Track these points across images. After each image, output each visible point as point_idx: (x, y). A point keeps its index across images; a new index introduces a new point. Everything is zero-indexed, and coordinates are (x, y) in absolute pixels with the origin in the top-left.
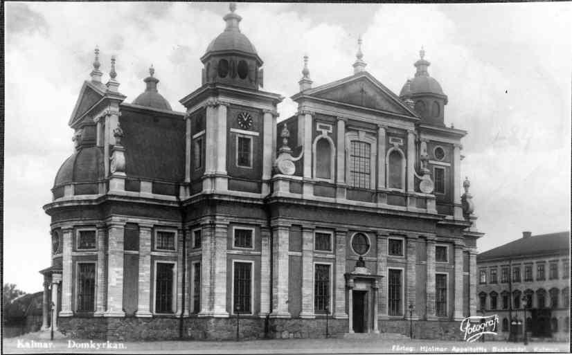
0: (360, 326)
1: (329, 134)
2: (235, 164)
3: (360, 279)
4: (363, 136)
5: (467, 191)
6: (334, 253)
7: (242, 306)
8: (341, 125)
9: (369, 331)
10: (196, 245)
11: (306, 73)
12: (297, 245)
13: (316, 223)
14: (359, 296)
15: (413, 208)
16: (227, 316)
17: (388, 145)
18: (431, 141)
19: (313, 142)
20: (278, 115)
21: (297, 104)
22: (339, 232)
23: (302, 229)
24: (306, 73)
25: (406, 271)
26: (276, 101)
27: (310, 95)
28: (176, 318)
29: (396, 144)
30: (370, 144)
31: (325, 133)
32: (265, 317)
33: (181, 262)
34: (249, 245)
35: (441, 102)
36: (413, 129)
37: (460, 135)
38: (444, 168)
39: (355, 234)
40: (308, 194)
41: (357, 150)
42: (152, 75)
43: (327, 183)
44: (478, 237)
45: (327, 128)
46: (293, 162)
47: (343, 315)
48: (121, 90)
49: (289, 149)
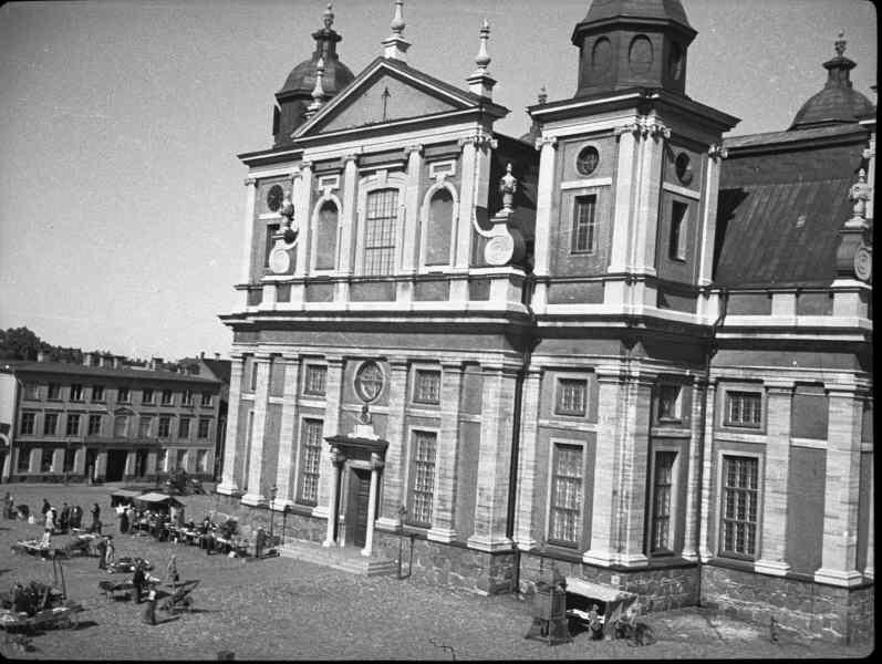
1: (334, 191)
4: (379, 179)
8: (351, 168)
12: (275, 389)
15: (458, 298)
17: (426, 181)
18: (559, 138)
19: (311, 213)
27: (305, 135)
29: (441, 175)
30: (397, 190)
31: (327, 196)
38: (598, 192)
40: (297, 301)
42: (840, 53)
45: (333, 181)
46: (287, 251)
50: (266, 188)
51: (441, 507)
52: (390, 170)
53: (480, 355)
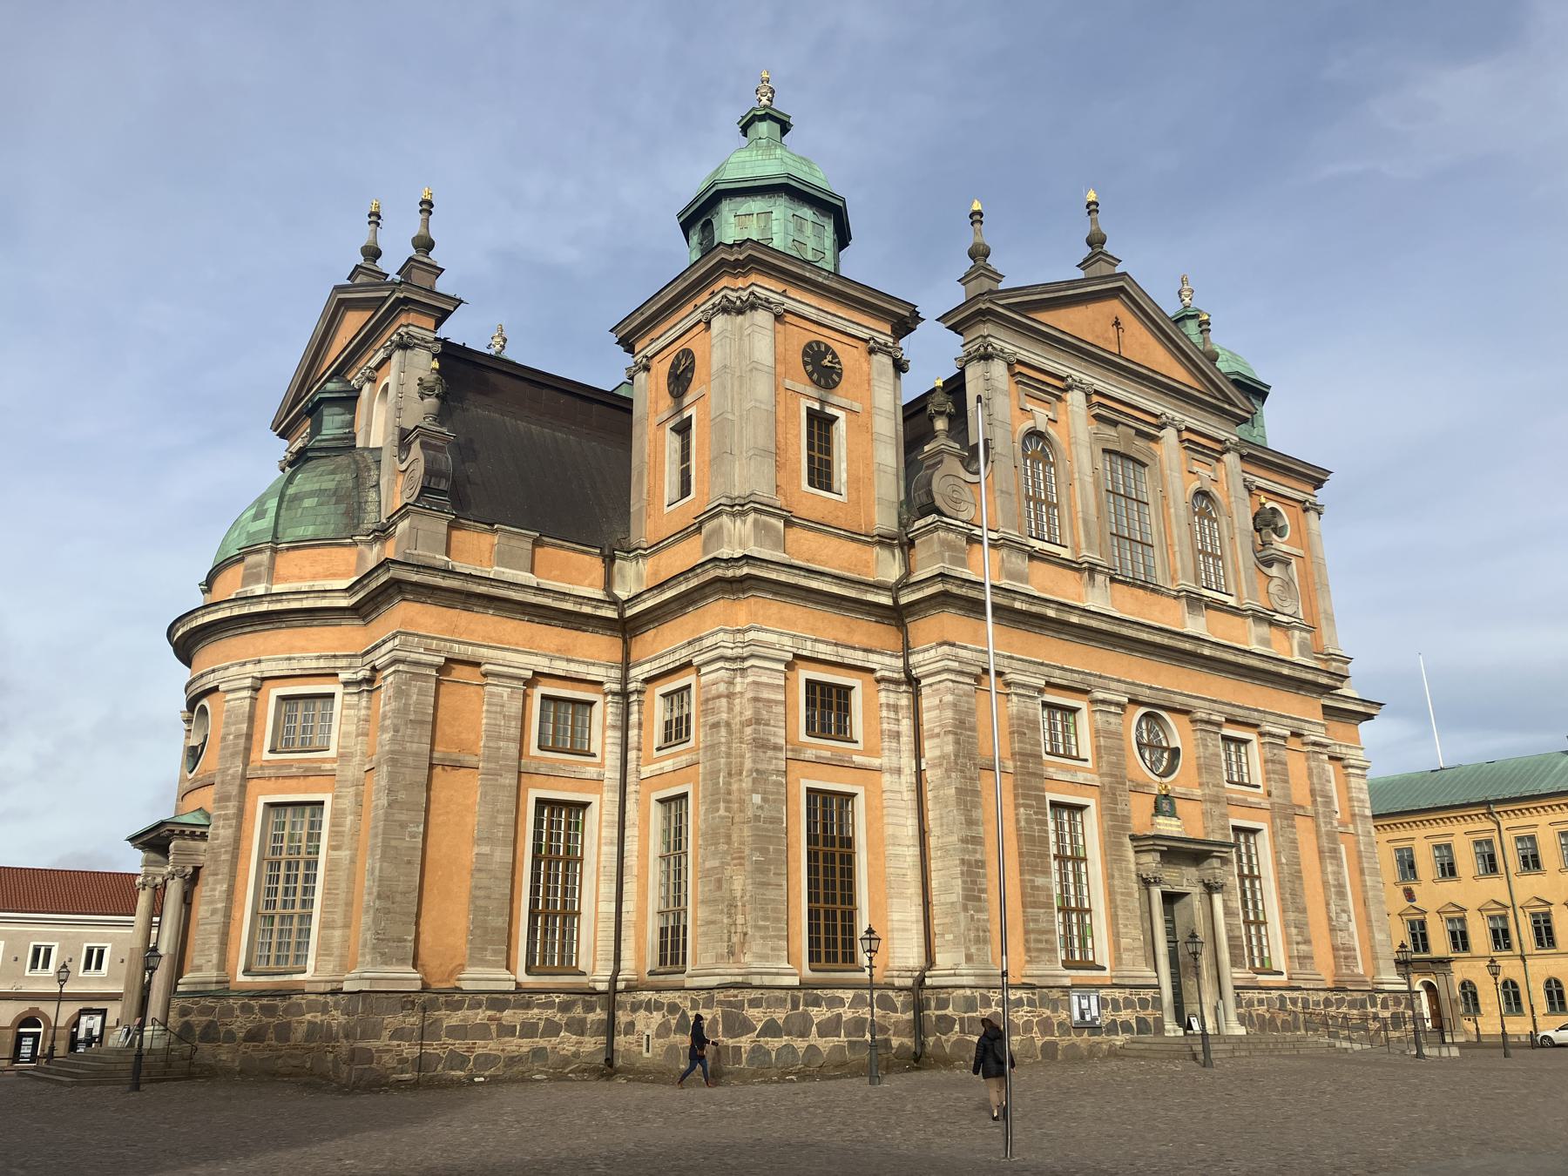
2: (799, 486)
7: (830, 943)
10: (667, 738)
13: (1045, 670)
16: (795, 981)
22: (1103, 702)
24: (979, 253)
25: (1274, 834)
26: (905, 322)
27: (1003, 306)
28: (594, 992)
32: (909, 982)
33: (611, 797)
34: (842, 732)
39: (1144, 710)
43: (1057, 556)
49: (958, 446)
50: (800, 336)
51: (1299, 939)
52: (1139, 433)
53: (1307, 726)
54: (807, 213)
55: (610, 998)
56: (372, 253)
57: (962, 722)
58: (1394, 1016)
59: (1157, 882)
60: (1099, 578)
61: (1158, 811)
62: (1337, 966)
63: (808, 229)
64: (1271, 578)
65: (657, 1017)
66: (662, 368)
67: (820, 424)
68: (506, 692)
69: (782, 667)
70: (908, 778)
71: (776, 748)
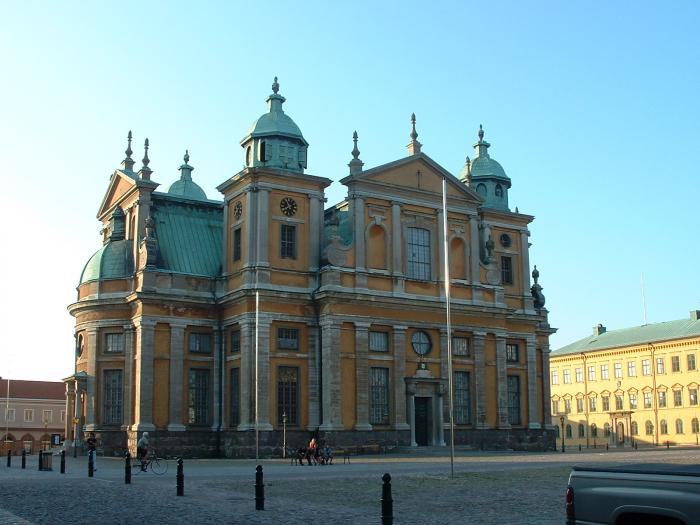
0: (423, 439)
3: (422, 382)
5: (536, 282)
6: (393, 355)
8: (396, 209)
9: (434, 442)
11: (356, 153)
14: (423, 403)
20: (326, 200)
21: (346, 188)
23: (355, 327)
24: (356, 153)
26: (326, 182)
35: (503, 187)
36: (476, 213)
37: (530, 219)
41: (415, 238)
44: (551, 333)
47: (404, 426)
48: (153, 178)
50: (280, 198)
54: (286, 144)
55: (218, 433)
56: (129, 152)
57: (334, 343)
58: (531, 438)
59: (413, 394)
60: (400, 282)
61: (419, 368)
62: (497, 422)
63: (286, 149)
64: (488, 270)
65: (230, 440)
66: (233, 205)
67: (288, 232)
68: (178, 333)
69: (268, 326)
70: (317, 361)
71: (266, 354)
